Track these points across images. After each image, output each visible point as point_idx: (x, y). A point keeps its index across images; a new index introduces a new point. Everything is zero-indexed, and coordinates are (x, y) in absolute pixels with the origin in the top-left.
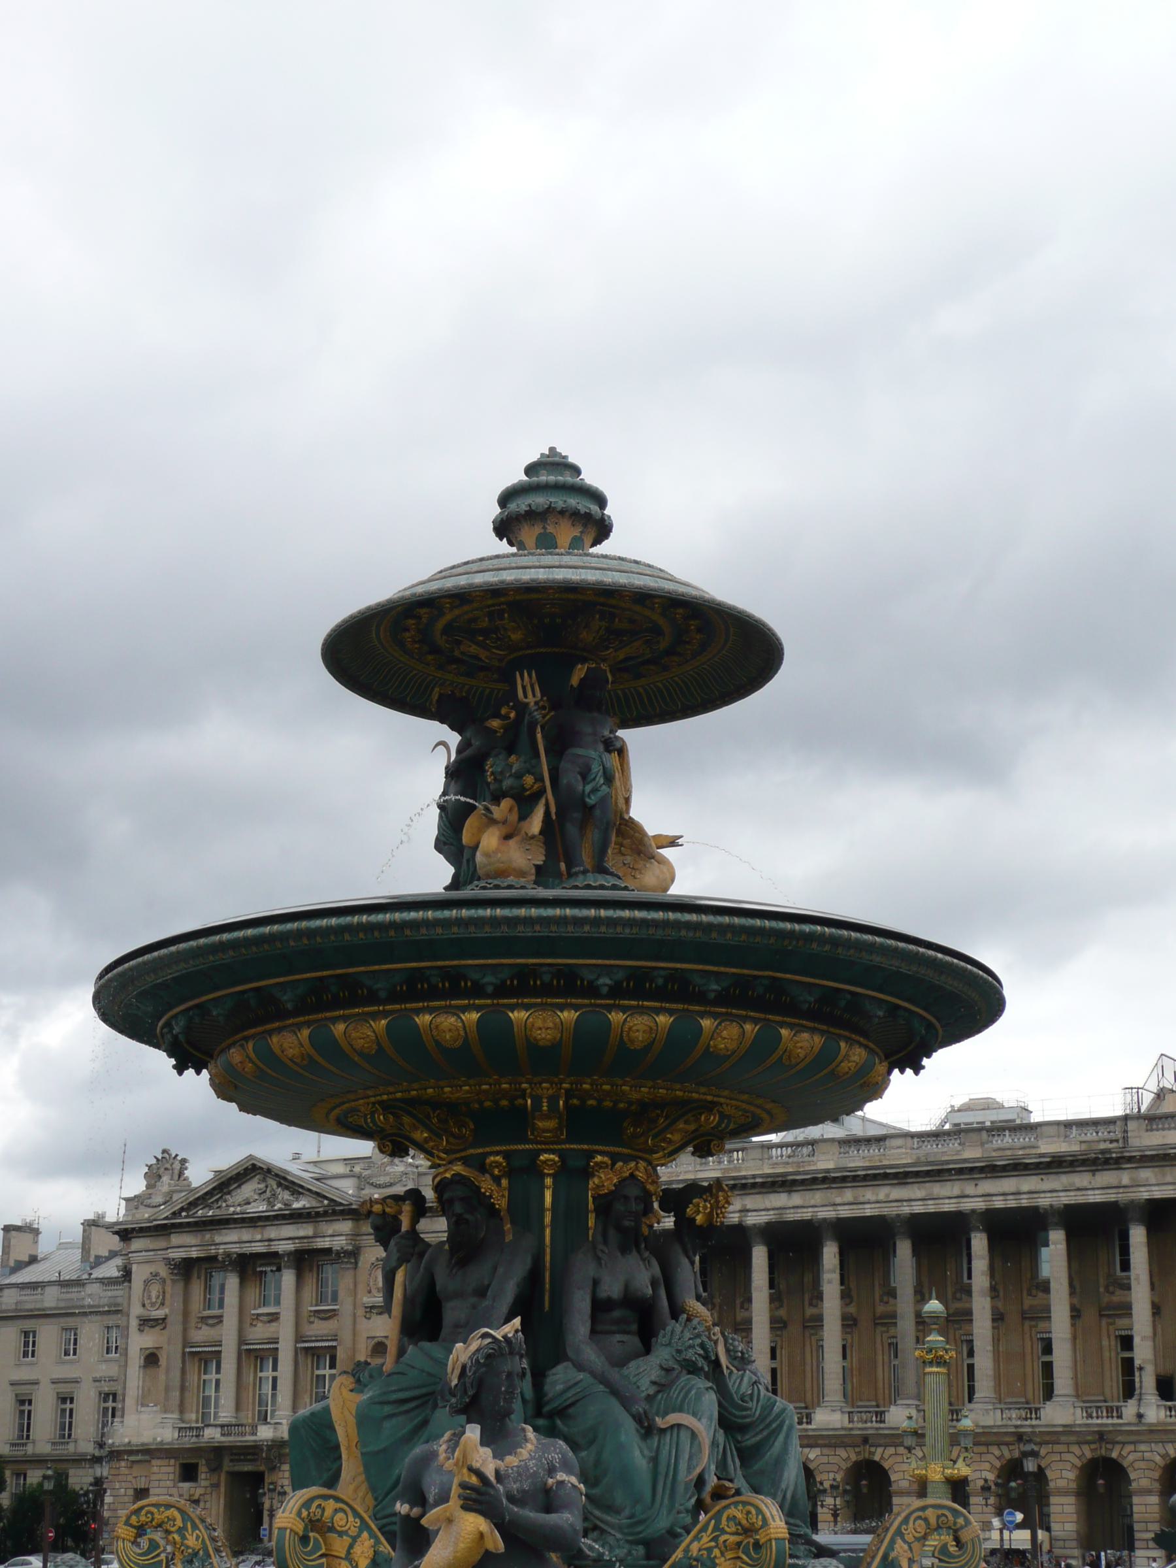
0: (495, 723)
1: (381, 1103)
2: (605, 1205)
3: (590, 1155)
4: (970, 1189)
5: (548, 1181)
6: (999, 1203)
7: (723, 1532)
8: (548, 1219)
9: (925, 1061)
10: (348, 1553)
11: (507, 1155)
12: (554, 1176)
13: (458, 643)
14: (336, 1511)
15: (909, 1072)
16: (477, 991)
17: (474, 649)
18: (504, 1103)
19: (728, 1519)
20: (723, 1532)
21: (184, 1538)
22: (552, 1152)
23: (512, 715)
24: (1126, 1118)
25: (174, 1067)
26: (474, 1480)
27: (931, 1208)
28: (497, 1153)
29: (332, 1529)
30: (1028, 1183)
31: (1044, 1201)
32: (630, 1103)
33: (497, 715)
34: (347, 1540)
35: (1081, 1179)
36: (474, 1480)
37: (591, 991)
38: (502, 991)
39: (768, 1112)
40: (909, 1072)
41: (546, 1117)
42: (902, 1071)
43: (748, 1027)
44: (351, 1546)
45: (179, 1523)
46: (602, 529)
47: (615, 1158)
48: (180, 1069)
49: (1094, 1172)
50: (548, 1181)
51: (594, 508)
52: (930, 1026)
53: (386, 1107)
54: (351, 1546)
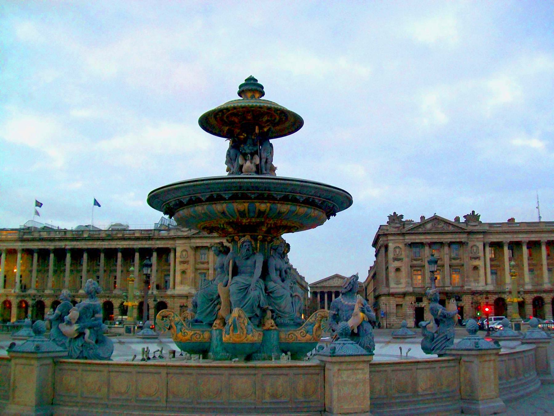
0: (242, 137)
4: (119, 243)
5: (259, 242)
6: (125, 247)
7: (317, 317)
19: (319, 315)
20: (317, 317)
21: (174, 319)
24: (155, 230)
27: (109, 247)
30: (132, 243)
31: (135, 247)
35: (144, 242)
46: (263, 94)
49: (146, 241)
51: (261, 89)
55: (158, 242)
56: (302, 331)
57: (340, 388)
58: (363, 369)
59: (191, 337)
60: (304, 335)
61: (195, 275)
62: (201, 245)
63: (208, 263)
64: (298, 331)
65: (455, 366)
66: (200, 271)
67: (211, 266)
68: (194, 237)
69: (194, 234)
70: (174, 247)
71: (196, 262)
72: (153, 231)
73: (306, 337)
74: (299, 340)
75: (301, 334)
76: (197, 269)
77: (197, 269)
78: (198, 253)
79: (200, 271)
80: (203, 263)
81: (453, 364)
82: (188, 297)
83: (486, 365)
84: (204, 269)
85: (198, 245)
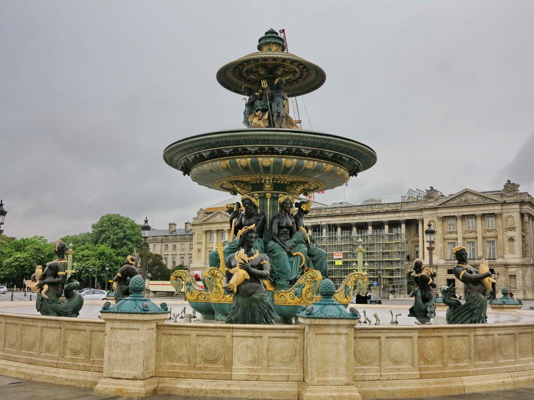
1: (229, 181)
2: (282, 205)
3: (278, 194)
4: (368, 217)
6: (375, 220)
8: (268, 209)
9: (358, 174)
10: (220, 282)
11: (259, 194)
12: (270, 199)
13: (249, 75)
14: (217, 272)
15: (354, 176)
16: (250, 153)
17: (252, 76)
18: (258, 182)
20: (307, 278)
21: (186, 279)
22: (270, 193)
23: (261, 92)
25: (183, 174)
26: (242, 262)
27: (360, 221)
28: (257, 193)
29: (216, 276)
30: (381, 216)
31: (384, 220)
32: (288, 182)
33: (258, 92)
34: (220, 279)
35: (392, 215)
36: (242, 262)
37: (278, 153)
38: (256, 153)
39: (320, 184)
40: (354, 176)
41: (268, 185)
42: (352, 176)
43: (316, 162)
44: (221, 280)
45: (185, 276)
47: (284, 194)
48: (184, 174)
50: (269, 200)
52: (359, 164)
53: (231, 182)
54: (221, 280)
55: (406, 214)
56: (291, 293)
57: (112, 349)
58: (139, 329)
59: (197, 297)
60: (292, 298)
61: (444, 245)
62: (448, 215)
63: (456, 232)
64: (288, 293)
65: (296, 338)
66: (449, 241)
67: (460, 236)
68: (440, 208)
69: (440, 205)
70: (422, 218)
71: (444, 233)
72: (400, 204)
73: (295, 300)
74: (289, 303)
75: (291, 296)
76: (445, 239)
77: (445, 239)
78: (446, 224)
79: (449, 241)
80: (451, 233)
81: (293, 335)
82: (438, 267)
83: (331, 339)
84: (453, 239)
85: (445, 215)
